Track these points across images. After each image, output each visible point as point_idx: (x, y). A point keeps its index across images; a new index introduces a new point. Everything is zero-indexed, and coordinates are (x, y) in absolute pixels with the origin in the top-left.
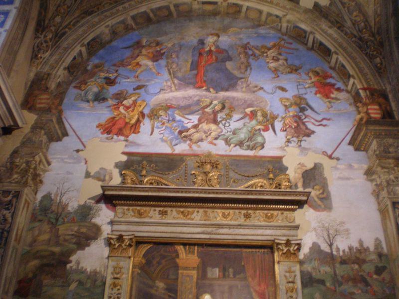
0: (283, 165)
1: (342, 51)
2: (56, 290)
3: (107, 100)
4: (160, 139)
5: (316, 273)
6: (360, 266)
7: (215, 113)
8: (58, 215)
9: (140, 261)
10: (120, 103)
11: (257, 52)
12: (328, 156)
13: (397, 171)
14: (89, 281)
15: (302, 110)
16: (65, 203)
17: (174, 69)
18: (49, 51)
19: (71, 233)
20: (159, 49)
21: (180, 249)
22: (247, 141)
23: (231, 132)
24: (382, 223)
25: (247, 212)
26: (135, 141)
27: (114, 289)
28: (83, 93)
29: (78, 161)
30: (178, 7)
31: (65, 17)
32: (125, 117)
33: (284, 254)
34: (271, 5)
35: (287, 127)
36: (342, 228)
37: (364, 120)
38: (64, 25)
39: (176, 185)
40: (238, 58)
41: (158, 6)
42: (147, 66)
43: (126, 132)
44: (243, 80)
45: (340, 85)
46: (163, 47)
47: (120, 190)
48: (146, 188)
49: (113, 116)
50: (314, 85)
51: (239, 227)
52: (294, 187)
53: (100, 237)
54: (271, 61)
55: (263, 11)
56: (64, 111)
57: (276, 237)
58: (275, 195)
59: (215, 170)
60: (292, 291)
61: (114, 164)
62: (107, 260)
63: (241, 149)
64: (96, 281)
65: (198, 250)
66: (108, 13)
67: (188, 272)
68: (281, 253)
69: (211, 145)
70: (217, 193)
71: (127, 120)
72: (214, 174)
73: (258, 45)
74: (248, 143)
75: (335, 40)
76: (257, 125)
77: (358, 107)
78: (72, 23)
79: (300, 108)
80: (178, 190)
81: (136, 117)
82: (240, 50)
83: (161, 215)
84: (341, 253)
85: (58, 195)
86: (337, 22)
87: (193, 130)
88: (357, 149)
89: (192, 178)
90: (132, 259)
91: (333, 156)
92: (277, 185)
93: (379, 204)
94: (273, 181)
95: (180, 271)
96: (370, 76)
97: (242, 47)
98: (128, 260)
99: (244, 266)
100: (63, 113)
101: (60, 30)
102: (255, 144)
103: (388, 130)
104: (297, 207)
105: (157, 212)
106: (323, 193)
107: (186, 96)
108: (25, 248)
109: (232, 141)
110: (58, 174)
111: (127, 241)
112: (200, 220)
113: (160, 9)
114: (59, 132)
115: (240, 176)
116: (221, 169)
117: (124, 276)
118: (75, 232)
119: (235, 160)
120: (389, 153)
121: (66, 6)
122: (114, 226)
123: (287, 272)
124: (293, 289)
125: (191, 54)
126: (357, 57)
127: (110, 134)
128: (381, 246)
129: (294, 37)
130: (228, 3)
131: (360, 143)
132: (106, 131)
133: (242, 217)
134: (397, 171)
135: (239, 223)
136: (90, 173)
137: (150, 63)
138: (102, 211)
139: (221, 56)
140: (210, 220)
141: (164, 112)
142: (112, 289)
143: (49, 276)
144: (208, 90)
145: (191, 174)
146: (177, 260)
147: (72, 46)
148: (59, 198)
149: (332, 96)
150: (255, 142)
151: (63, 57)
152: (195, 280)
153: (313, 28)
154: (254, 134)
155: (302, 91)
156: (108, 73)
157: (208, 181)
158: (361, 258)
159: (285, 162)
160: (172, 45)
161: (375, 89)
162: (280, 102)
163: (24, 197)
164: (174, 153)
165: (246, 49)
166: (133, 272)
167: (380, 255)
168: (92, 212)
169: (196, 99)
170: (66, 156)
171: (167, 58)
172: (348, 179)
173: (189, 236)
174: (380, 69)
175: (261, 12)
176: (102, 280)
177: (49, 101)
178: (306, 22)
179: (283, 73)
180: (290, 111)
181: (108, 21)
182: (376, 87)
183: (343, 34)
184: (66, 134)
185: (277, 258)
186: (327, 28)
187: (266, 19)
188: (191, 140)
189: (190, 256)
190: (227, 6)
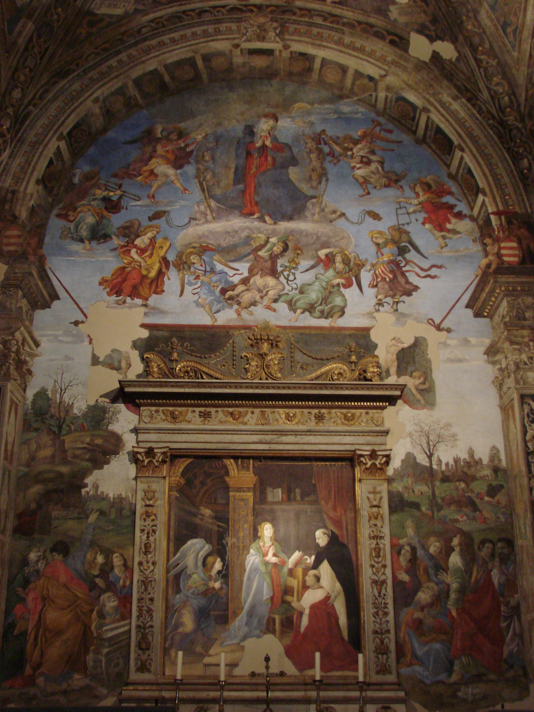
1: (470, 144)
3: (111, 238)
4: (195, 302)
5: (409, 493)
6: (467, 485)
7: (274, 258)
8: (60, 421)
9: (179, 481)
10: (130, 244)
11: (337, 149)
12: (435, 326)
13: (532, 348)
15: (402, 251)
16: (68, 404)
17: (208, 181)
18: (8, 149)
19: (81, 446)
20: (183, 145)
21: (230, 463)
22: (321, 304)
23: (296, 289)
24: (503, 427)
25: (319, 412)
28: (72, 226)
29: (78, 338)
30: (209, 60)
31: (28, 88)
32: (140, 266)
33: (367, 469)
34: (361, 56)
35: (379, 280)
36: (447, 433)
37: (493, 266)
38: (26, 102)
40: (308, 160)
41: (176, 59)
42: (166, 176)
43: (144, 291)
44: (314, 200)
45: (462, 207)
46: (189, 141)
49: (123, 265)
50: (423, 207)
51: (308, 433)
54: (358, 166)
55: (348, 68)
56: (48, 258)
57: (357, 447)
58: (357, 389)
59: (274, 350)
60: (376, 518)
61: (131, 344)
63: (311, 316)
64: (121, 510)
66: (93, 74)
67: (242, 494)
68: (363, 467)
70: (279, 388)
71: (144, 272)
72: (273, 358)
73: (338, 135)
74: (321, 308)
75: (462, 123)
76: (335, 277)
77: (485, 245)
78: (37, 96)
79: (399, 248)
80: (225, 384)
81: (157, 266)
82: (311, 145)
84: (444, 467)
85: (56, 391)
86: (467, 90)
87: (241, 288)
88: (477, 315)
90: (167, 479)
91: (442, 326)
93: (501, 397)
94: (355, 366)
95: (231, 494)
96: (510, 190)
97: (313, 140)
99: (314, 485)
100: (48, 261)
101: (20, 111)
102: (332, 309)
103: (526, 282)
105: (197, 413)
106: (424, 383)
107: (229, 230)
108: (22, 468)
109: (299, 304)
110: (53, 360)
111: (159, 455)
112: (257, 424)
113: (179, 64)
114: (46, 296)
115: (310, 359)
116: (284, 348)
117: (158, 502)
119: (302, 334)
120: (525, 319)
121: (28, 69)
123: (370, 493)
124: (378, 515)
125: (234, 154)
126: (494, 154)
127: (120, 296)
128: (498, 457)
129: (395, 119)
130: (291, 52)
131: (483, 303)
132: (114, 291)
133: (313, 418)
134: (532, 348)
135: (309, 428)
137: (171, 171)
138: (121, 414)
139: (280, 157)
141: (198, 257)
142: (145, 520)
144: (261, 219)
145: (241, 358)
146: (227, 479)
147: (43, 140)
149: (449, 226)
150: (331, 305)
151: (32, 161)
152: (251, 504)
153: (428, 100)
154: (330, 293)
155: (404, 219)
156: (107, 189)
158: (469, 473)
159: (374, 336)
160: (203, 138)
161: (516, 213)
162: (370, 239)
163: (9, 396)
164: (215, 324)
165: (320, 144)
166: (169, 496)
167: (496, 470)
168: (107, 415)
169: (244, 234)
170: (61, 333)
171: (197, 162)
172: (460, 361)
173: (242, 447)
174: (527, 178)
175: (344, 69)
177: (21, 240)
178: (416, 90)
179: (375, 187)
180: (384, 253)
181: (96, 90)
182: (517, 209)
183: (475, 111)
184: (55, 297)
185: (358, 475)
186: (450, 100)
187: (353, 84)
188: (239, 303)
190: (290, 59)
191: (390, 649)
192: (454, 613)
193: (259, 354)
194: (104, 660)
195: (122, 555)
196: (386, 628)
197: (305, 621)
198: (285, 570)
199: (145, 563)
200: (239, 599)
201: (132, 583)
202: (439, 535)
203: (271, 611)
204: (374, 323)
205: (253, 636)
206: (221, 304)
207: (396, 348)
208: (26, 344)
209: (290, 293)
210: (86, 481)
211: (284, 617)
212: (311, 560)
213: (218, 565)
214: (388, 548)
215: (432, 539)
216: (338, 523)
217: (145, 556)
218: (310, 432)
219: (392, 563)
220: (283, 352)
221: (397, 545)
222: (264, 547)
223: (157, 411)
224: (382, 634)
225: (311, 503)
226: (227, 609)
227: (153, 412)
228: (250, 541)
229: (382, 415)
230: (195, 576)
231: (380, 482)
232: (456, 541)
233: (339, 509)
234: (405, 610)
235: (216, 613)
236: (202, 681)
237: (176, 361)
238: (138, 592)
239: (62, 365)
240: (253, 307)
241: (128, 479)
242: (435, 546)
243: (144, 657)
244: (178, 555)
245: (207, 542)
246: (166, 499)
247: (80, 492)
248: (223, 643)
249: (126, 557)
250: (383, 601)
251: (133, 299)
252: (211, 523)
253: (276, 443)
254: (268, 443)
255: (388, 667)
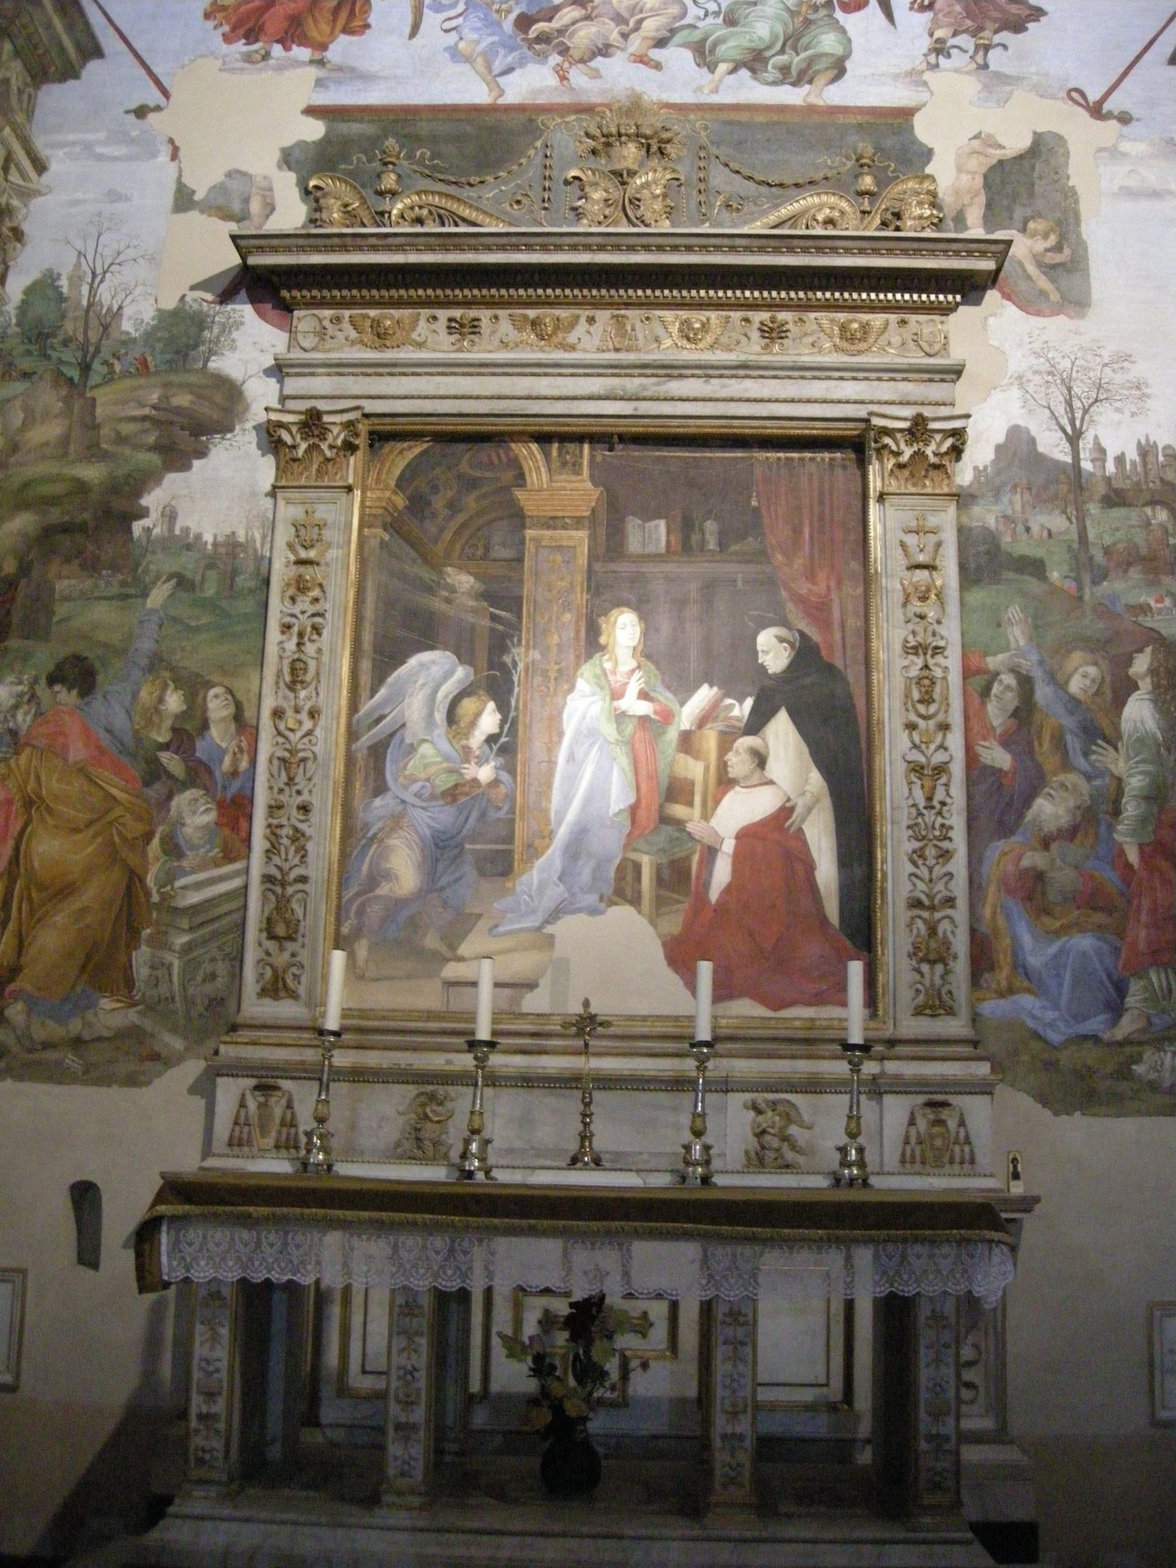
0: (914, 141)
2: (103, 615)
4: (447, 49)
12: (1087, 107)
14: (212, 574)
16: (110, 309)
21: (530, 454)
22: (782, 51)
23: (717, 14)
26: (352, 63)
27: (299, 599)
33: (901, 466)
36: (1119, 378)
39: (511, 224)
47: (302, 249)
48: (396, 235)
51: (741, 372)
52: (951, 224)
53: (241, 421)
57: (875, 408)
58: (876, 252)
59: (654, 162)
60: (924, 598)
61: (277, 156)
62: (269, 502)
63: (755, 79)
64: (234, 573)
65: (592, 458)
68: (890, 463)
69: (641, 66)
70: (660, 249)
80: (514, 240)
83: (457, 336)
84: (1110, 467)
85: (81, 279)
89: (566, 197)
90: (358, 493)
91: (1106, 107)
92: (890, 217)
95: (529, 533)
98: (343, 497)
99: (756, 510)
102: (811, 61)
104: (958, 298)
106: (1058, 248)
109: (721, 50)
110: (76, 203)
111: (336, 430)
112: (600, 350)
115: (751, 184)
117: (332, 554)
118: (154, 407)
119: (730, 123)
122: (287, 380)
124: (928, 590)
127: (256, 40)
132: (241, 31)
133: (755, 335)
135: (743, 358)
136: (194, 192)
138: (242, 328)
140: (638, 350)
142: (293, 599)
143: (76, 562)
145: (567, 183)
146: (519, 494)
148: (85, 290)
152: (583, 561)
154: (808, 23)
157: (630, 206)
159: (923, 129)
164: (500, 101)
168: (206, 334)
170: (101, 136)
172: (1156, 194)
176: (258, 569)
184: (92, 50)
185: (875, 483)
188: (564, 51)
189: (565, 480)
191: (954, 949)
192: (1133, 856)
193: (613, 172)
194: (177, 964)
195: (230, 691)
196: (945, 893)
197: (722, 873)
198: (672, 735)
199: (290, 713)
200: (546, 812)
201: (253, 762)
202: (1095, 646)
203: (630, 843)
204: (924, 96)
205: (579, 910)
206: (516, 54)
207: (982, 158)
208: (13, 170)
209: (700, 24)
210: (146, 501)
211: (664, 860)
212: (742, 709)
213: (489, 721)
214: (955, 678)
215: (1077, 657)
216: (818, 611)
217: (292, 695)
218: (744, 369)
219: (967, 719)
220: (678, 167)
221: (978, 672)
222: (614, 673)
223: (337, 320)
224: (932, 908)
225: (747, 559)
226: (510, 839)
227: (326, 323)
228: (578, 657)
229: (945, 327)
230: (426, 749)
231: (938, 503)
232: (1141, 664)
233: (822, 575)
234: (1001, 845)
235: (478, 847)
236: (434, 1025)
237: (394, 194)
238: (271, 788)
239: (100, 214)
240: (599, 58)
241: (253, 494)
242: (1085, 676)
243: (281, 959)
244: (382, 692)
245: (462, 660)
246: (353, 547)
247: (129, 530)
248: (496, 926)
249: (239, 696)
250: (940, 820)
251: (287, 48)
252: (475, 611)
253: (651, 399)
254: (630, 399)
255: (945, 997)
